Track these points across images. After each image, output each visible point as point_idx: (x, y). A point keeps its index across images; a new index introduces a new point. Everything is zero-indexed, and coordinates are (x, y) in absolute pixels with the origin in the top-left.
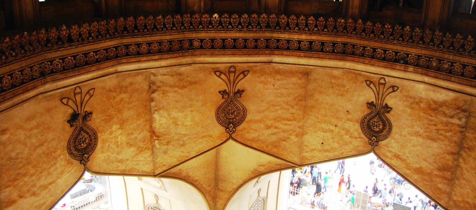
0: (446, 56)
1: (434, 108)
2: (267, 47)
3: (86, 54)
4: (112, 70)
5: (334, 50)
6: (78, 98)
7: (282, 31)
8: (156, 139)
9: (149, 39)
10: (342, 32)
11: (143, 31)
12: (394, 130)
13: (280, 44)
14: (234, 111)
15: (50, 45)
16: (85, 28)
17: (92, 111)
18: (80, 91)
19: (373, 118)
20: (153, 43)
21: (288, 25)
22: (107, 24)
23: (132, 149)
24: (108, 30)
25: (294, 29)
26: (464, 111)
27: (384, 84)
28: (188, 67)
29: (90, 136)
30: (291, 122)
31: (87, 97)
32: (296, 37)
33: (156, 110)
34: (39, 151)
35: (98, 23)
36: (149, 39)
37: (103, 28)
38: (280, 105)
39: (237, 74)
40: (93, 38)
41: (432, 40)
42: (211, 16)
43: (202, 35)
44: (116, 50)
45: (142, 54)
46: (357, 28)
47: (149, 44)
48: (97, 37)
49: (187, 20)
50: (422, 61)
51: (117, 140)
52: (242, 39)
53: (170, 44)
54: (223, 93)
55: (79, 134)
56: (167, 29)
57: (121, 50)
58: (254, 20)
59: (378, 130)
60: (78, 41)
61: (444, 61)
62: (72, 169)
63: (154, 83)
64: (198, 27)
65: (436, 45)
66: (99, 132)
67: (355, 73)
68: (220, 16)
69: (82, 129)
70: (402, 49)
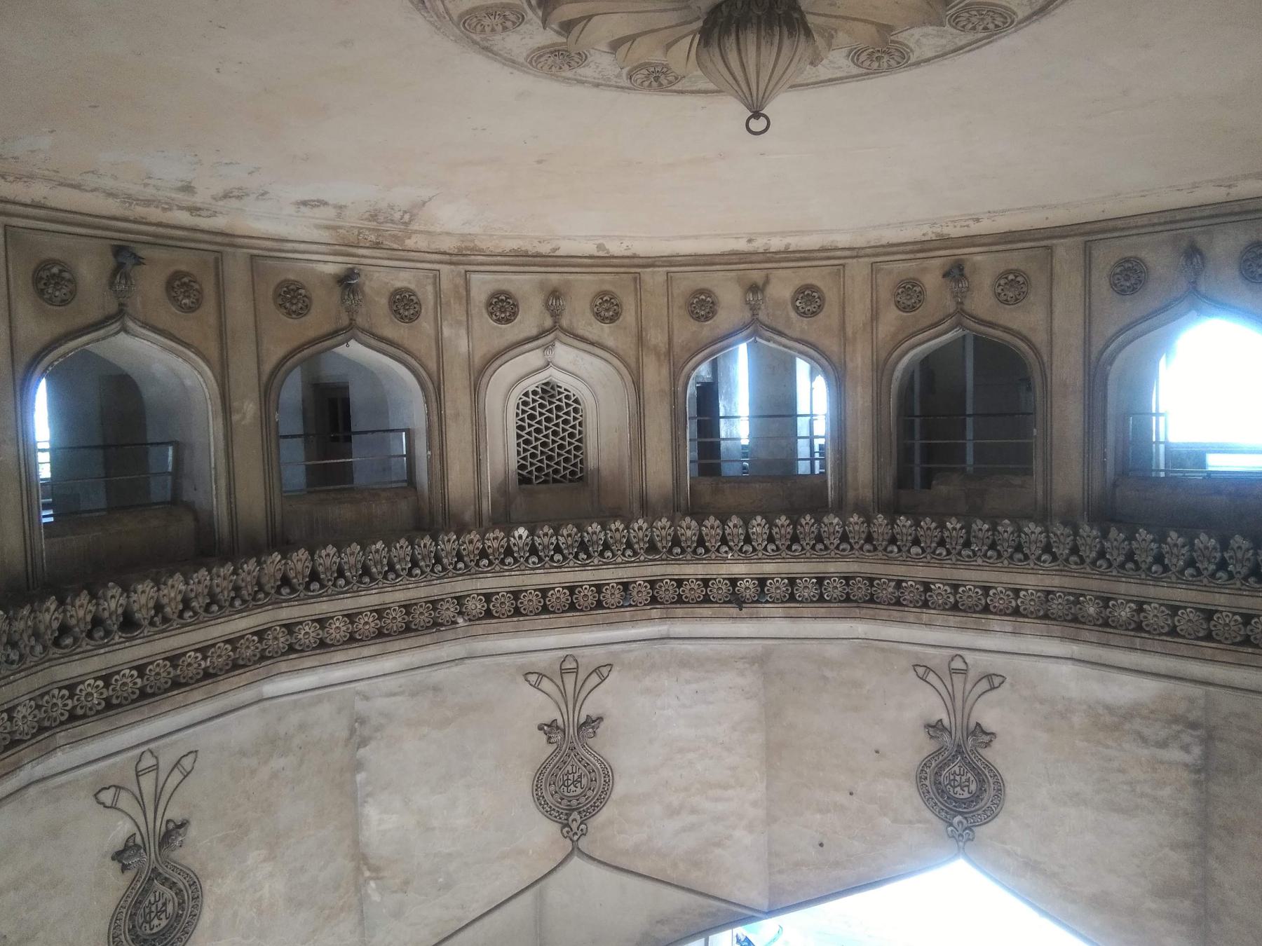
0: (1122, 588)
1: (1114, 722)
2: (654, 600)
3: (174, 659)
4: (247, 695)
5: (821, 595)
6: (147, 783)
7: (689, 557)
8: (371, 878)
9: (349, 604)
10: (837, 548)
11: (334, 585)
12: (1011, 791)
13: (685, 590)
14: (580, 777)
15: (69, 641)
16: (173, 586)
17: (186, 817)
18: (152, 762)
19: (947, 765)
20: (361, 613)
21: (701, 542)
22: (235, 573)
24: (237, 589)
25: (718, 550)
26: (1194, 726)
27: (964, 672)
29: (179, 893)
30: (730, 793)
31: (177, 776)
35: (210, 571)
36: (349, 604)
37: (225, 584)
39: (582, 676)
40: (195, 613)
41: (1075, 550)
42: (509, 534)
44: (260, 641)
45: (333, 645)
46: (875, 535)
47: (351, 617)
48: (207, 609)
49: (448, 547)
50: (1056, 606)
51: (258, 895)
53: (408, 613)
54: (549, 728)
55: (145, 892)
56: (398, 576)
57: (276, 638)
58: (618, 535)
59: (966, 795)
60: (152, 624)
61: (1116, 600)
63: (362, 721)
64: (477, 565)
65: (1088, 560)
67: (883, 650)
68: (532, 533)
69: (155, 874)
70: (1000, 578)
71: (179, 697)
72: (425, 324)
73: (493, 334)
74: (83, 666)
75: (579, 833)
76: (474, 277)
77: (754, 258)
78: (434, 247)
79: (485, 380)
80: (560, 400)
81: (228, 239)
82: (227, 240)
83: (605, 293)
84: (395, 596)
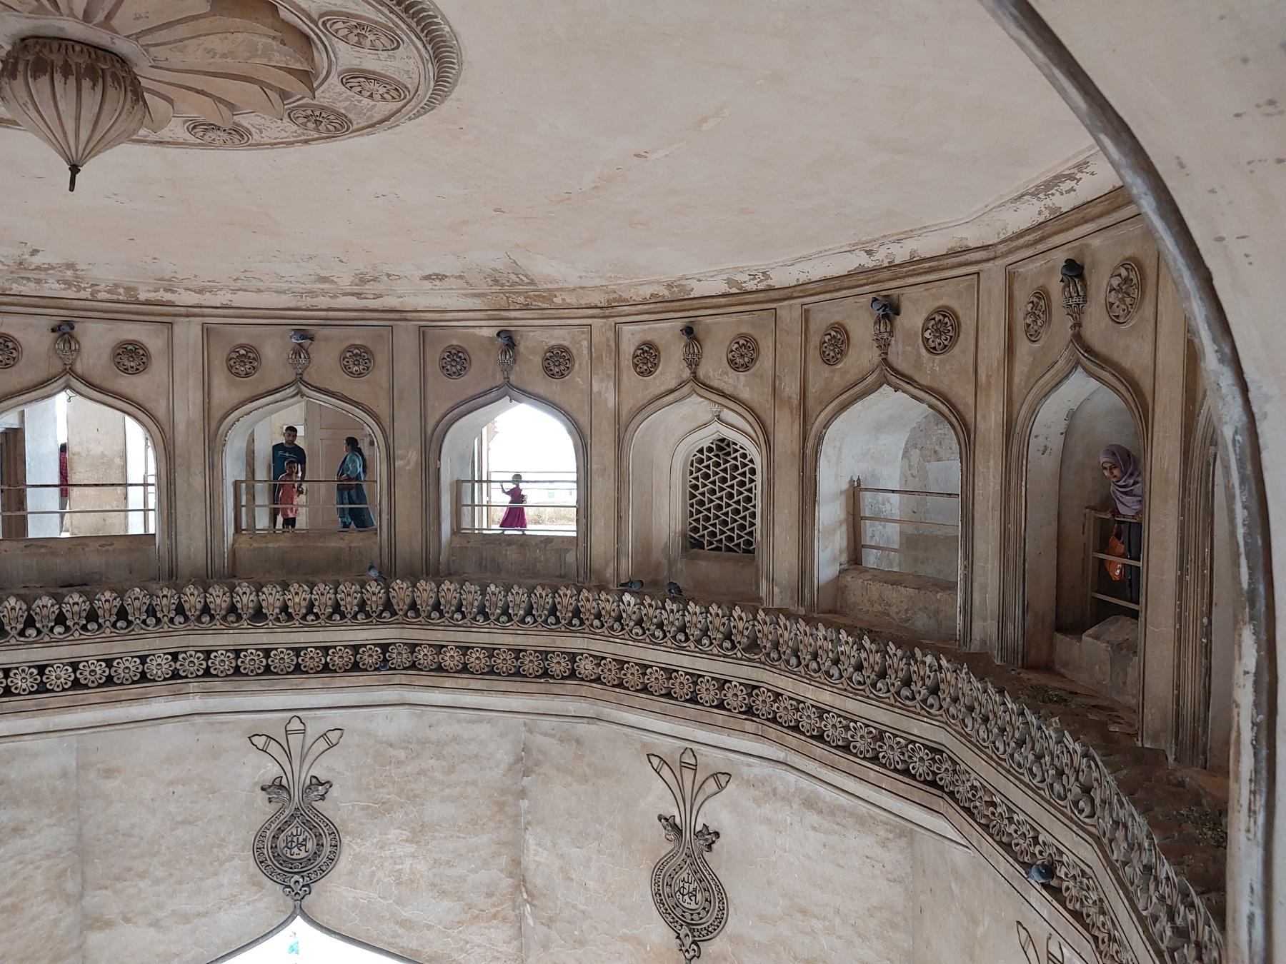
2: (750, 712)
10: (925, 701)
14: (695, 890)
23: (447, 903)
28: (593, 727)
31: (322, 745)
32: (810, 692)
33: (529, 823)
34: (179, 832)
38: (824, 918)
43: (598, 646)
47: (465, 650)
48: (330, 617)
49: (565, 601)
52: (687, 673)
53: (517, 658)
56: (510, 619)
60: (278, 619)
62: (261, 899)
66: (347, 833)
71: (296, 680)
72: (578, 377)
73: (638, 388)
74: (221, 639)
75: (692, 953)
76: (626, 328)
77: (881, 276)
78: (583, 302)
79: (628, 435)
80: (735, 459)
81: (401, 314)
82: (397, 316)
83: (742, 336)
84: (506, 638)
